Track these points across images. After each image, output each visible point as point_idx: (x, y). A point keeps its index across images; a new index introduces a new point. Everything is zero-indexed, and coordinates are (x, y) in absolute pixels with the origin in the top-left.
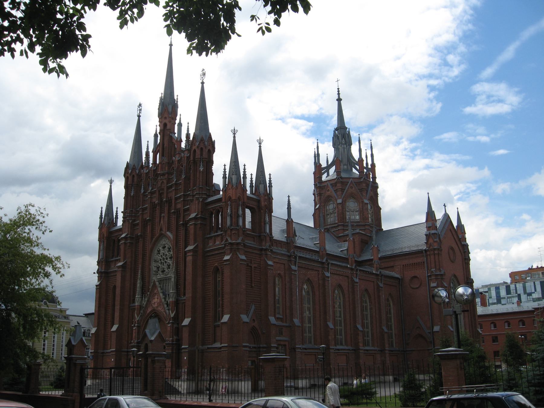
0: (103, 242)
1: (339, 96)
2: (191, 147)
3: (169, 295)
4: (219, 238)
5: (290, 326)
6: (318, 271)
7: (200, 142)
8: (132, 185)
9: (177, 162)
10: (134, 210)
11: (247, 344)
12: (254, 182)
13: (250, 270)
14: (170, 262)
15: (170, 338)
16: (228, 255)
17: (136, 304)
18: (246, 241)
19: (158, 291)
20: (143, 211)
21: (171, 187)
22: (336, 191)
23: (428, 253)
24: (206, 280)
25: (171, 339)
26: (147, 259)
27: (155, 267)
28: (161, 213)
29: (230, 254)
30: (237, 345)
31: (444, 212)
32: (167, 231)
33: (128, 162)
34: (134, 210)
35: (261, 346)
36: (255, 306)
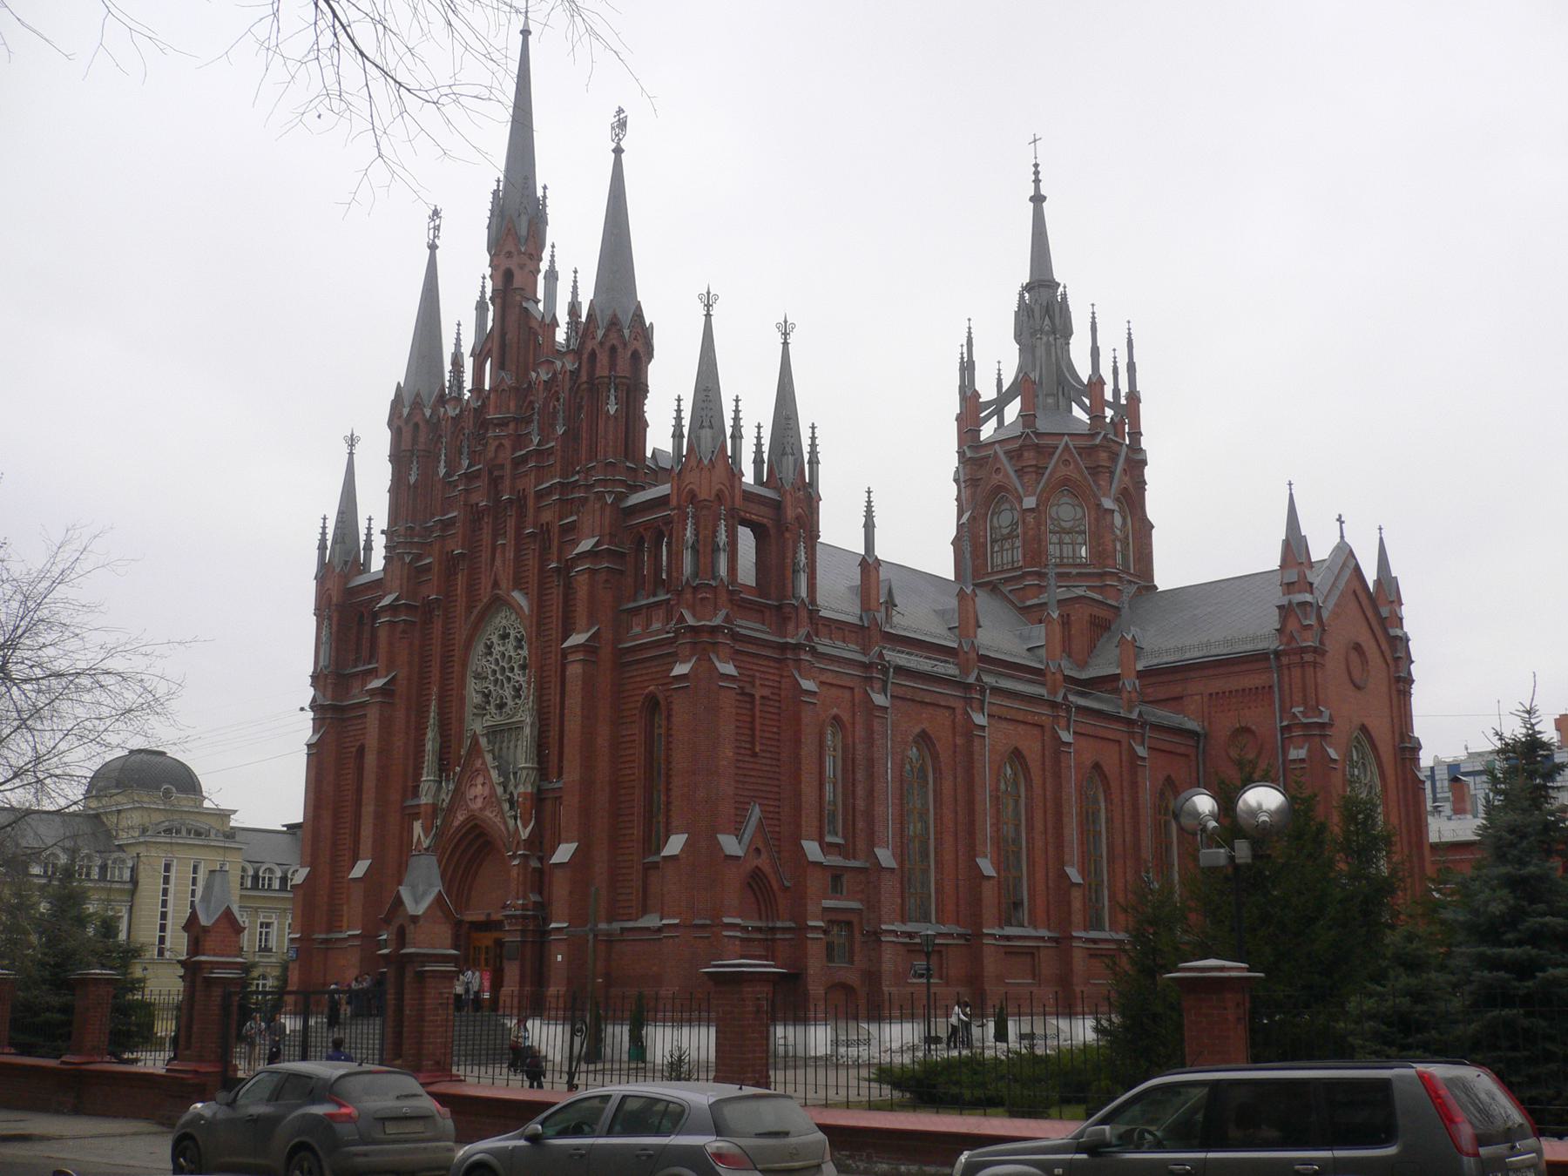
0: (330, 618)
1: (1037, 188)
2: (582, 344)
3: (515, 774)
4: (661, 612)
5: (867, 869)
6: (954, 709)
7: (608, 330)
8: (412, 451)
9: (541, 387)
10: (418, 528)
11: (738, 921)
12: (766, 449)
13: (748, 706)
14: (521, 679)
15: (518, 899)
16: (683, 662)
17: (424, 800)
18: (739, 622)
19: (484, 763)
20: (443, 530)
21: (524, 459)
22: (1020, 472)
23: (1285, 660)
24: (624, 733)
25: (520, 902)
26: (456, 668)
27: (477, 692)
28: (494, 539)
29: (689, 661)
30: (708, 922)
31: (1338, 540)
32: (513, 590)
33: (399, 384)
34: (418, 528)
35: (779, 924)
36: (761, 811)
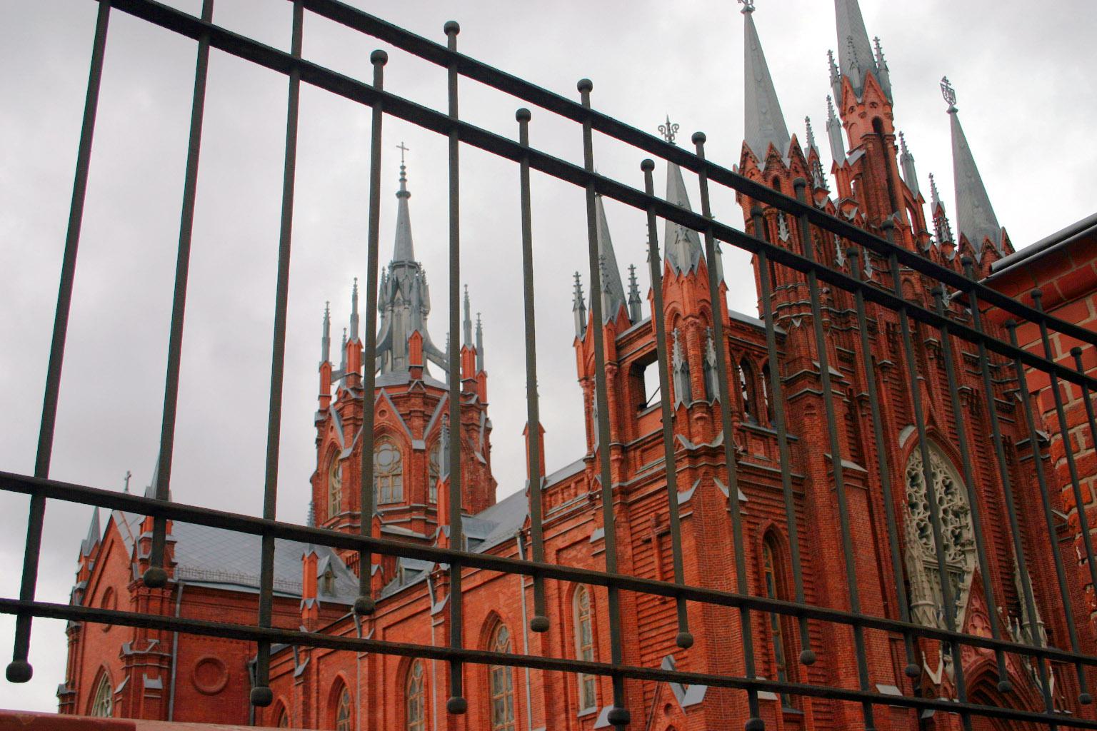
1: (403, 186)
22: (407, 417)
